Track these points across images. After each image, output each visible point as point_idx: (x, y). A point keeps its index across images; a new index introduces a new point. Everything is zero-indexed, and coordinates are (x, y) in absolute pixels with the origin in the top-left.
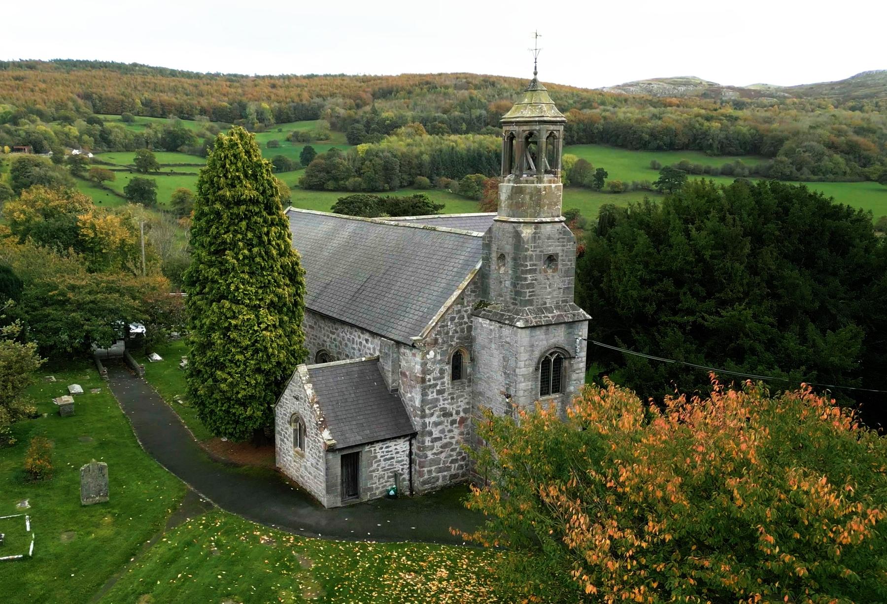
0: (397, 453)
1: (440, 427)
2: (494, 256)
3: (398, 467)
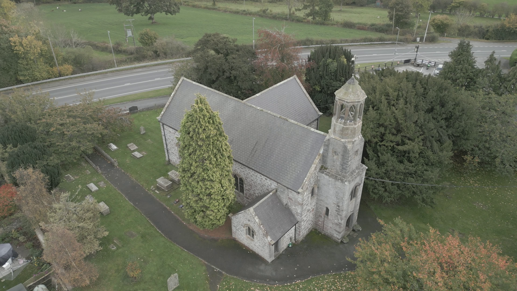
2: (330, 151)
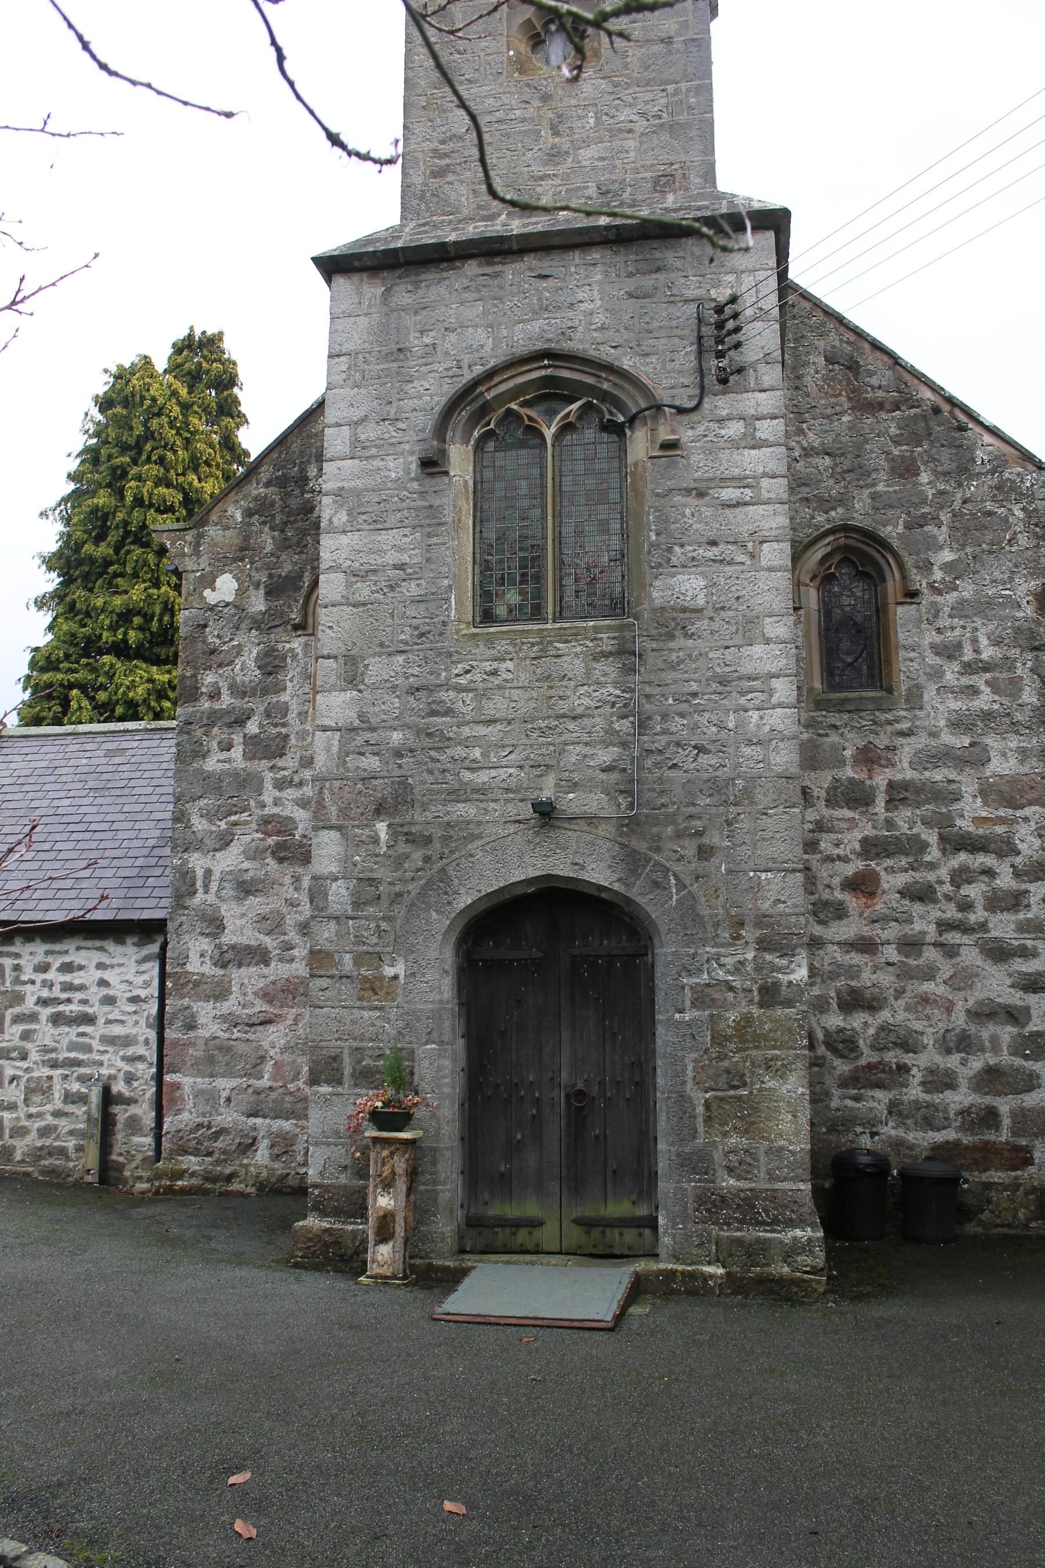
0: (110, 1001)
1: (256, 904)
3: (112, 1064)
